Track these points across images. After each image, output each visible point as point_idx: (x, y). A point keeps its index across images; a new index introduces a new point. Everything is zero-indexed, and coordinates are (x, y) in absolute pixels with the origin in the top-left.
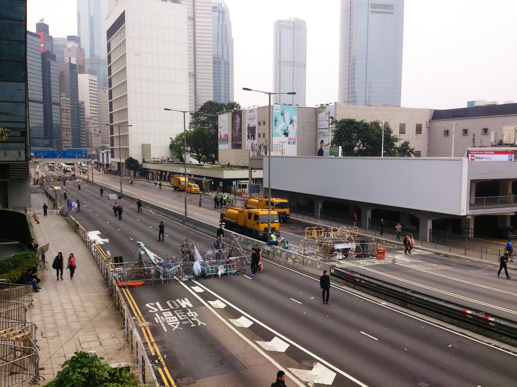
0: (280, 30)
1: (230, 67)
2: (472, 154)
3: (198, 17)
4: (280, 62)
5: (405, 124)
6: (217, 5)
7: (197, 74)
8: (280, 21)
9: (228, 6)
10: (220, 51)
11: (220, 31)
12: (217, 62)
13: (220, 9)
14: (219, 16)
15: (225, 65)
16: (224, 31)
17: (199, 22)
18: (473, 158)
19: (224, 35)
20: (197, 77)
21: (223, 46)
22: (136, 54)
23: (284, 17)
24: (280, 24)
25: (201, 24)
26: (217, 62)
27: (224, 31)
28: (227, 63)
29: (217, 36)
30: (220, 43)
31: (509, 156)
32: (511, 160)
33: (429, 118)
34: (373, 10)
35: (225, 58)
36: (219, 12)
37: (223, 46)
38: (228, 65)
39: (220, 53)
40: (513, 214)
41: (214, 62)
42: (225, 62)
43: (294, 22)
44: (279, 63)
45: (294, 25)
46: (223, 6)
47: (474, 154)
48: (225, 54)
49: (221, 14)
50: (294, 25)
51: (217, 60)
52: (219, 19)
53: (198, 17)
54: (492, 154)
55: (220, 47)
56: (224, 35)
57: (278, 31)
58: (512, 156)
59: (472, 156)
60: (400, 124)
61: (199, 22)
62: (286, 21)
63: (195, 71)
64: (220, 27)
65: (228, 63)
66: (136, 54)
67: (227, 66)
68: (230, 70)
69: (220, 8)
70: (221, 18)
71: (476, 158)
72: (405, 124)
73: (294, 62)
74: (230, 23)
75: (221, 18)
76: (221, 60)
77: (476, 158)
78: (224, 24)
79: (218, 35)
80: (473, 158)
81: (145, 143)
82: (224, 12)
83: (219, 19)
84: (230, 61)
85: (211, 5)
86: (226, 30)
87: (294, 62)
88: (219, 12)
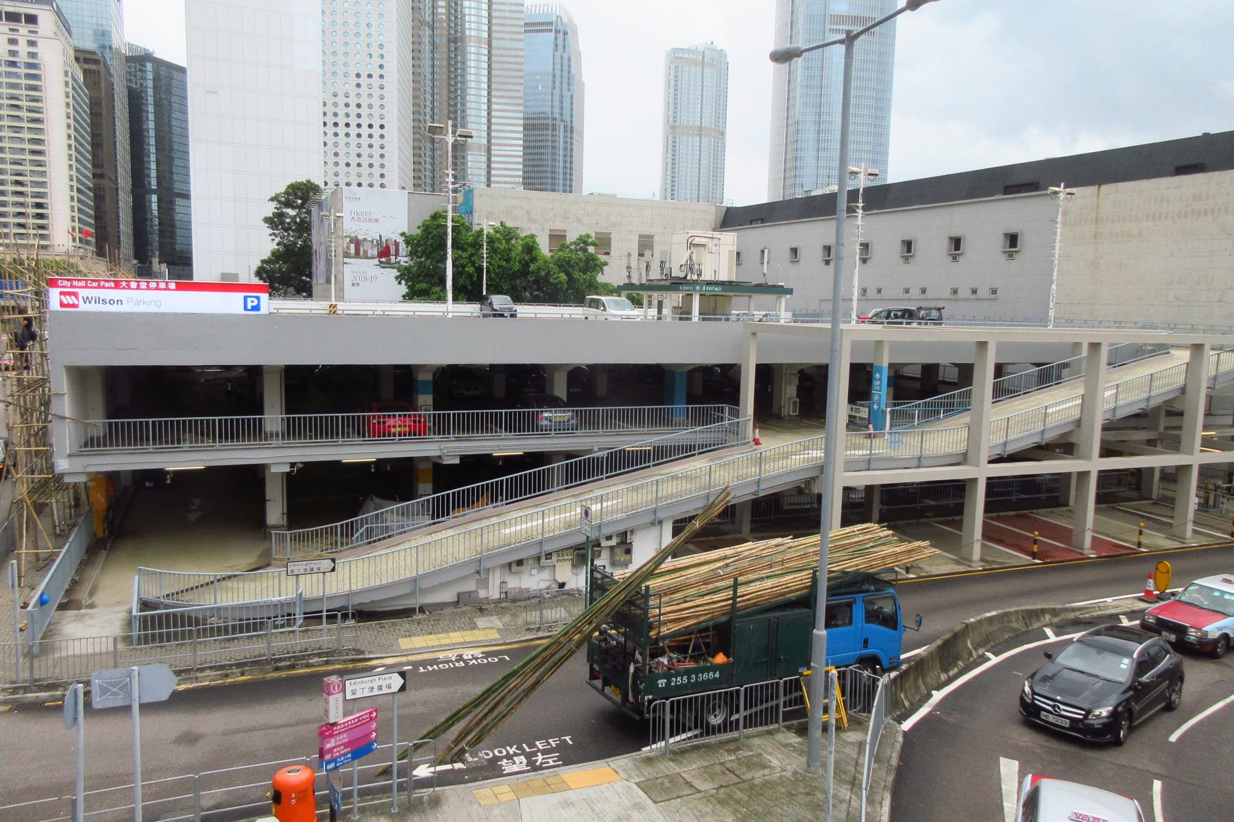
0: (677, 67)
1: (575, 136)
2: (63, 287)
3: (497, 39)
4: (673, 128)
5: (651, 237)
6: (554, 19)
7: (493, 148)
8: (675, 51)
9: (576, 21)
10: (557, 104)
11: (558, 67)
12: (550, 127)
13: (560, 27)
14: (556, 38)
15: (565, 131)
16: (565, 68)
17: (499, 48)
18: (68, 300)
19: (565, 73)
20: (493, 152)
21: (562, 96)
22: (207, 92)
23: (686, 41)
24: (677, 55)
25: (502, 52)
26: (550, 127)
27: (565, 68)
28: (569, 129)
29: (550, 78)
30: (557, 91)
31: (245, 298)
32: (256, 308)
33: (713, 225)
34: (835, 27)
35: (567, 118)
36: (557, 32)
37: (562, 96)
38: (572, 132)
39: (557, 110)
40: (457, 461)
41: (527, 127)
42: (565, 127)
43: (704, 52)
44: (674, 130)
45: (703, 57)
46: (565, 20)
47: (72, 286)
48: (567, 112)
49: (560, 35)
50: (703, 57)
51: (550, 121)
52: (556, 45)
53: (497, 39)
54: (111, 288)
55: (557, 98)
56: (565, 73)
57: (673, 68)
58: (258, 298)
59: (62, 293)
60: (640, 236)
61: (499, 48)
62: (689, 51)
63: (489, 141)
64: (558, 60)
65: (572, 128)
66: (207, 92)
67: (569, 134)
68: (574, 142)
69: (559, 24)
70: (560, 42)
71: (87, 300)
72: (651, 237)
73: (701, 128)
74: (579, 55)
75: (560, 42)
76: (558, 122)
77: (87, 300)
78: (565, 55)
79: (554, 76)
80: (68, 300)
81: (226, 271)
82: (565, 33)
83: (556, 45)
84: (575, 125)
85: (522, 16)
86: (569, 66)
87: (701, 128)
88: (557, 32)
